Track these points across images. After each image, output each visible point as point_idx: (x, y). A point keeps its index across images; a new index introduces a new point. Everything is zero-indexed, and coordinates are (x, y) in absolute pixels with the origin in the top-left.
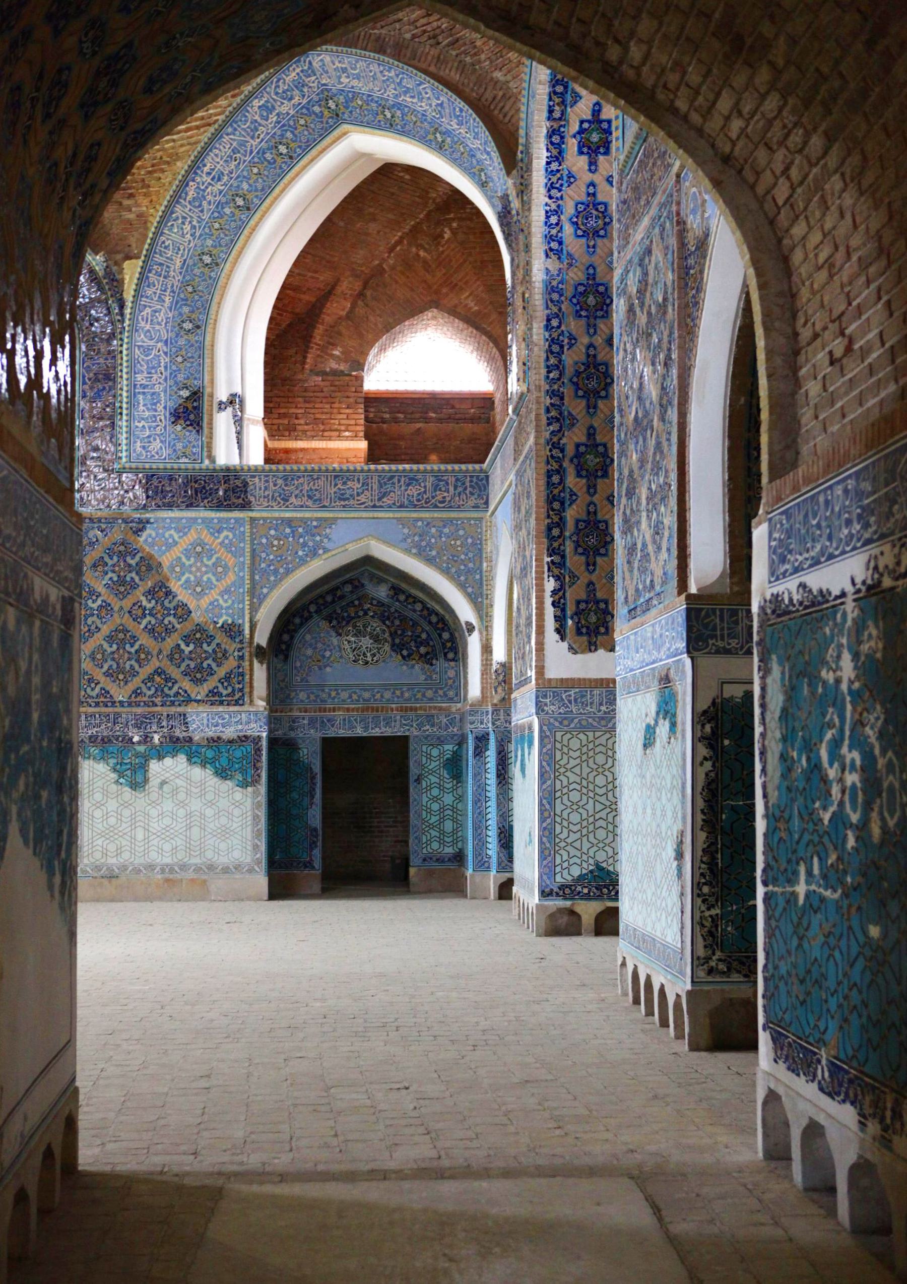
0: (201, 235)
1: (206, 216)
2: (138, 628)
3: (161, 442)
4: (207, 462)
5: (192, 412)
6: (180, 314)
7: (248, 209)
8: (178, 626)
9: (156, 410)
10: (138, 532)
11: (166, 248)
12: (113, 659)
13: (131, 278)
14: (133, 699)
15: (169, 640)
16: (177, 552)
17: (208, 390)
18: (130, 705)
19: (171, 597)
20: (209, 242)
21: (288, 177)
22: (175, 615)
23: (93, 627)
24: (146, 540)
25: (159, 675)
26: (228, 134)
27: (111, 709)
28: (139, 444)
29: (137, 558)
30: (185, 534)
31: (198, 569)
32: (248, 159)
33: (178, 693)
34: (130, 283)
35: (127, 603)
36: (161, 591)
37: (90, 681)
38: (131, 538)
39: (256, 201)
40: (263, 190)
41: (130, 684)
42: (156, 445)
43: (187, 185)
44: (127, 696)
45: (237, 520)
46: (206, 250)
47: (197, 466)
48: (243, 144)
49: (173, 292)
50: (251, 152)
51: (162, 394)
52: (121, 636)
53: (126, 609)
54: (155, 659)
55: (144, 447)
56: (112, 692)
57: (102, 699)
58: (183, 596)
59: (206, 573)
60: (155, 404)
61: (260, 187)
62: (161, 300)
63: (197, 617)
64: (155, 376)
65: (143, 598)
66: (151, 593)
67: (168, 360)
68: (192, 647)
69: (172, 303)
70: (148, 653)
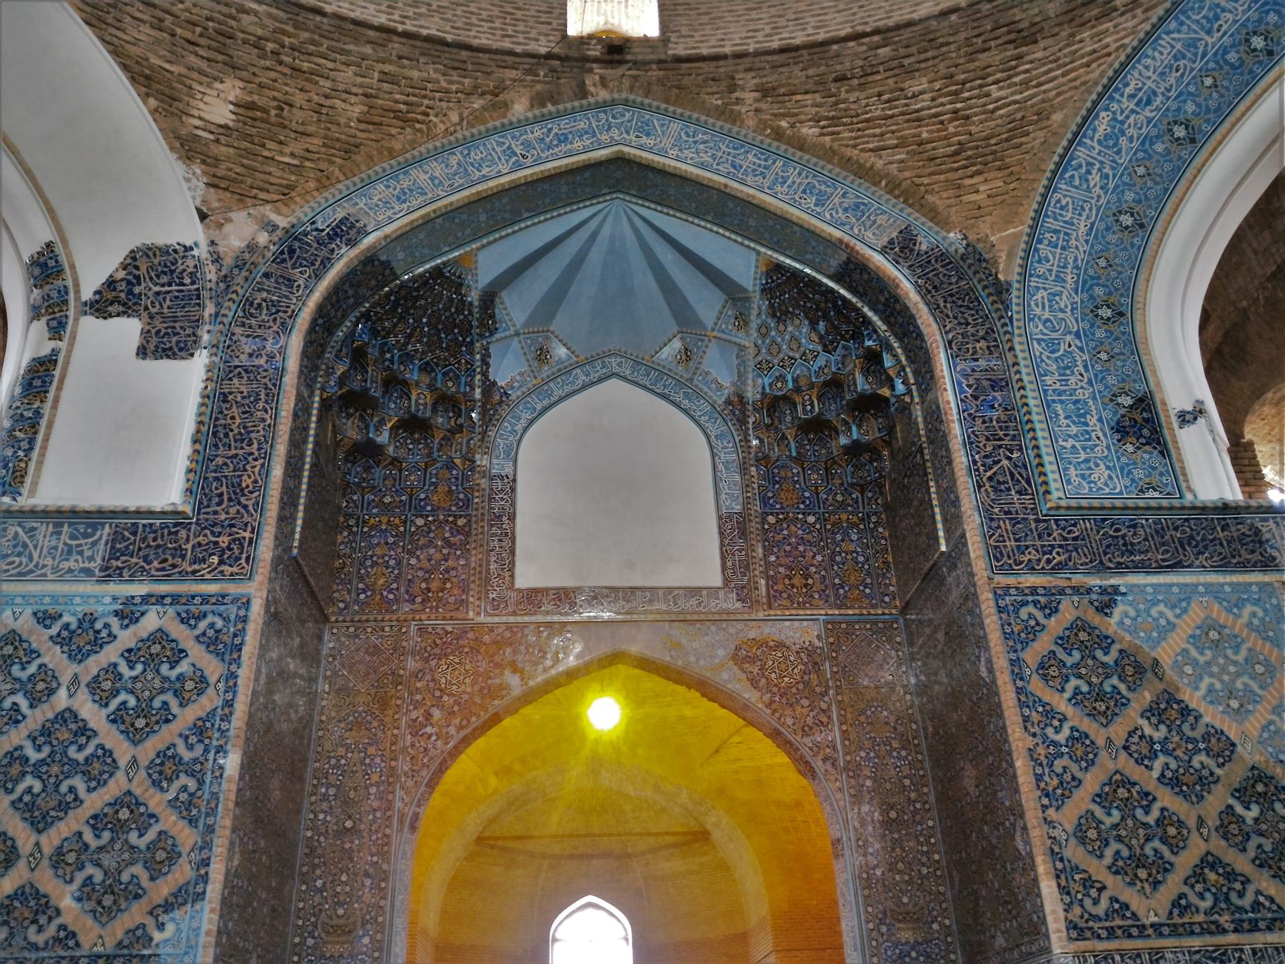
0: (1117, 186)
1: (1124, 159)
2: (1148, 778)
3: (1108, 468)
4: (1189, 497)
5: (1142, 424)
6: (1091, 297)
7: (1193, 141)
8: (1218, 772)
9: (1087, 424)
10: (1105, 608)
11: (1062, 208)
12: (1119, 839)
13: (1010, 255)
14: (1177, 920)
15: (1210, 798)
16: (1177, 641)
17: (1157, 398)
18: (1175, 931)
19: (1191, 719)
20: (1129, 196)
21: (1263, 84)
22: (1208, 751)
23: (1067, 777)
24: (1121, 623)
25: (1212, 867)
26: (1168, 33)
27: (1139, 944)
28: (1072, 471)
29: (1114, 653)
30: (1185, 611)
31: (1223, 670)
32: (1197, 66)
33: (1256, 905)
34: (1008, 265)
35: (1118, 731)
36: (1168, 708)
37: (1088, 883)
38: (1095, 619)
39: (1206, 128)
40: (1218, 109)
41: (1162, 888)
42: (1101, 473)
43: (1097, 117)
44: (1163, 913)
45: (1263, 586)
46: (1125, 206)
47: (1176, 503)
48: (1191, 44)
49: (1077, 267)
50: (1204, 54)
51: (1091, 403)
52: (1122, 792)
53: (1119, 742)
54: (1195, 836)
55: (1083, 476)
56: (1133, 907)
57: (1118, 922)
58: (1212, 716)
59: (1238, 675)
60: (1083, 416)
61: (1213, 104)
62: (1059, 279)
63: (1249, 754)
64: (1073, 379)
65: (1144, 723)
66: (1154, 712)
67: (1086, 357)
68: (1255, 811)
69: (1077, 283)
70: (1180, 824)
